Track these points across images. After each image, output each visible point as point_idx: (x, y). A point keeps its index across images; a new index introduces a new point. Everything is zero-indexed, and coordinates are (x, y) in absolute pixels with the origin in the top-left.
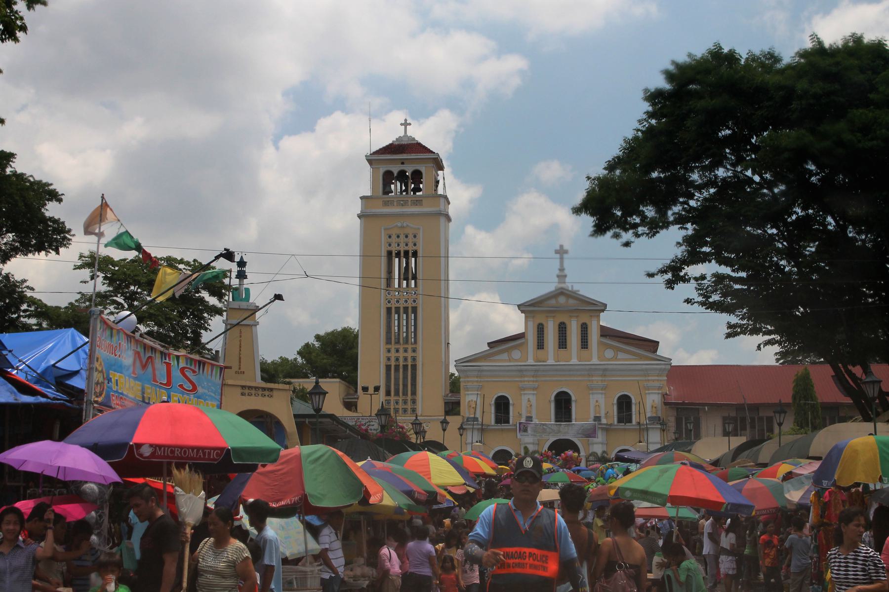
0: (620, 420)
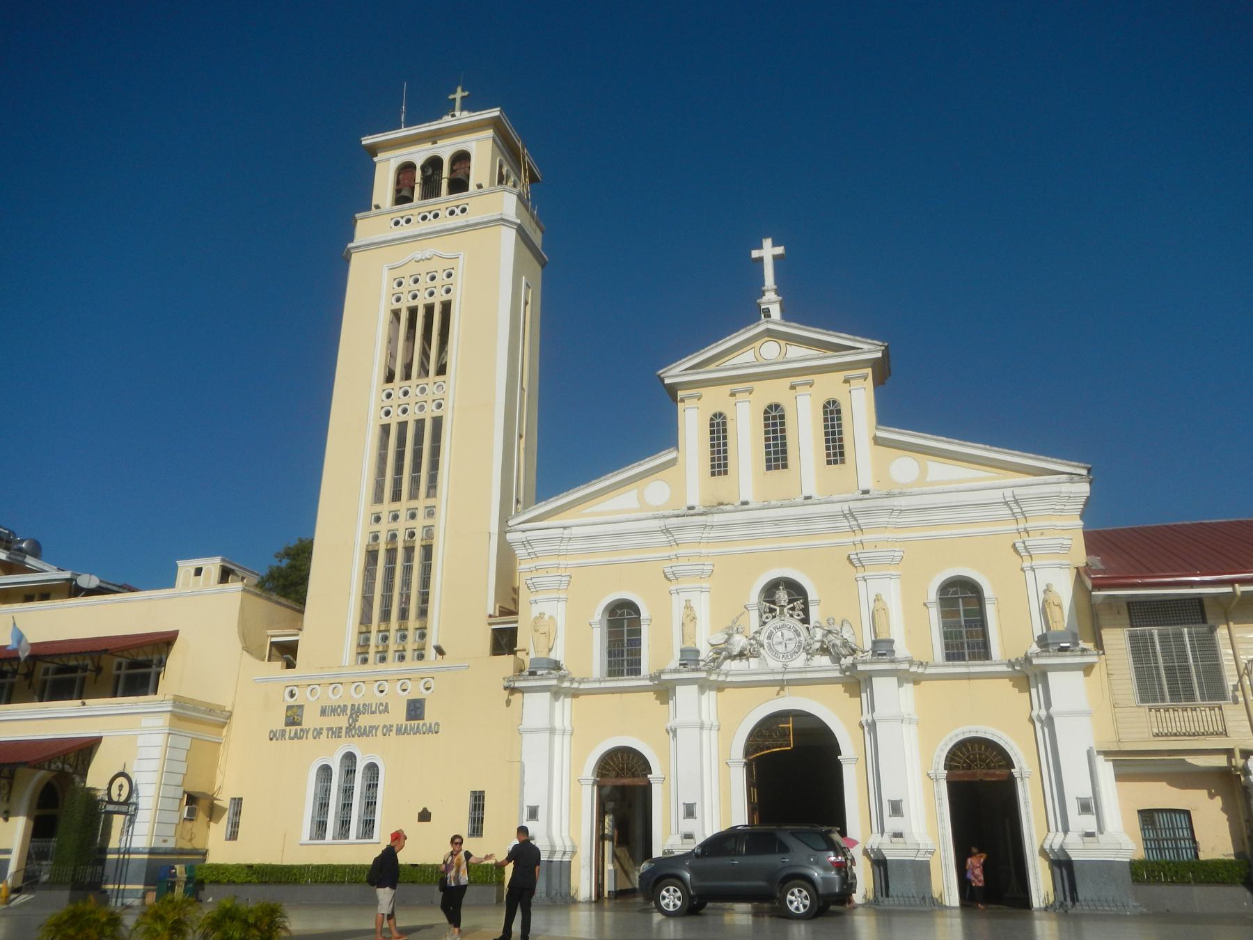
0: (953, 654)
